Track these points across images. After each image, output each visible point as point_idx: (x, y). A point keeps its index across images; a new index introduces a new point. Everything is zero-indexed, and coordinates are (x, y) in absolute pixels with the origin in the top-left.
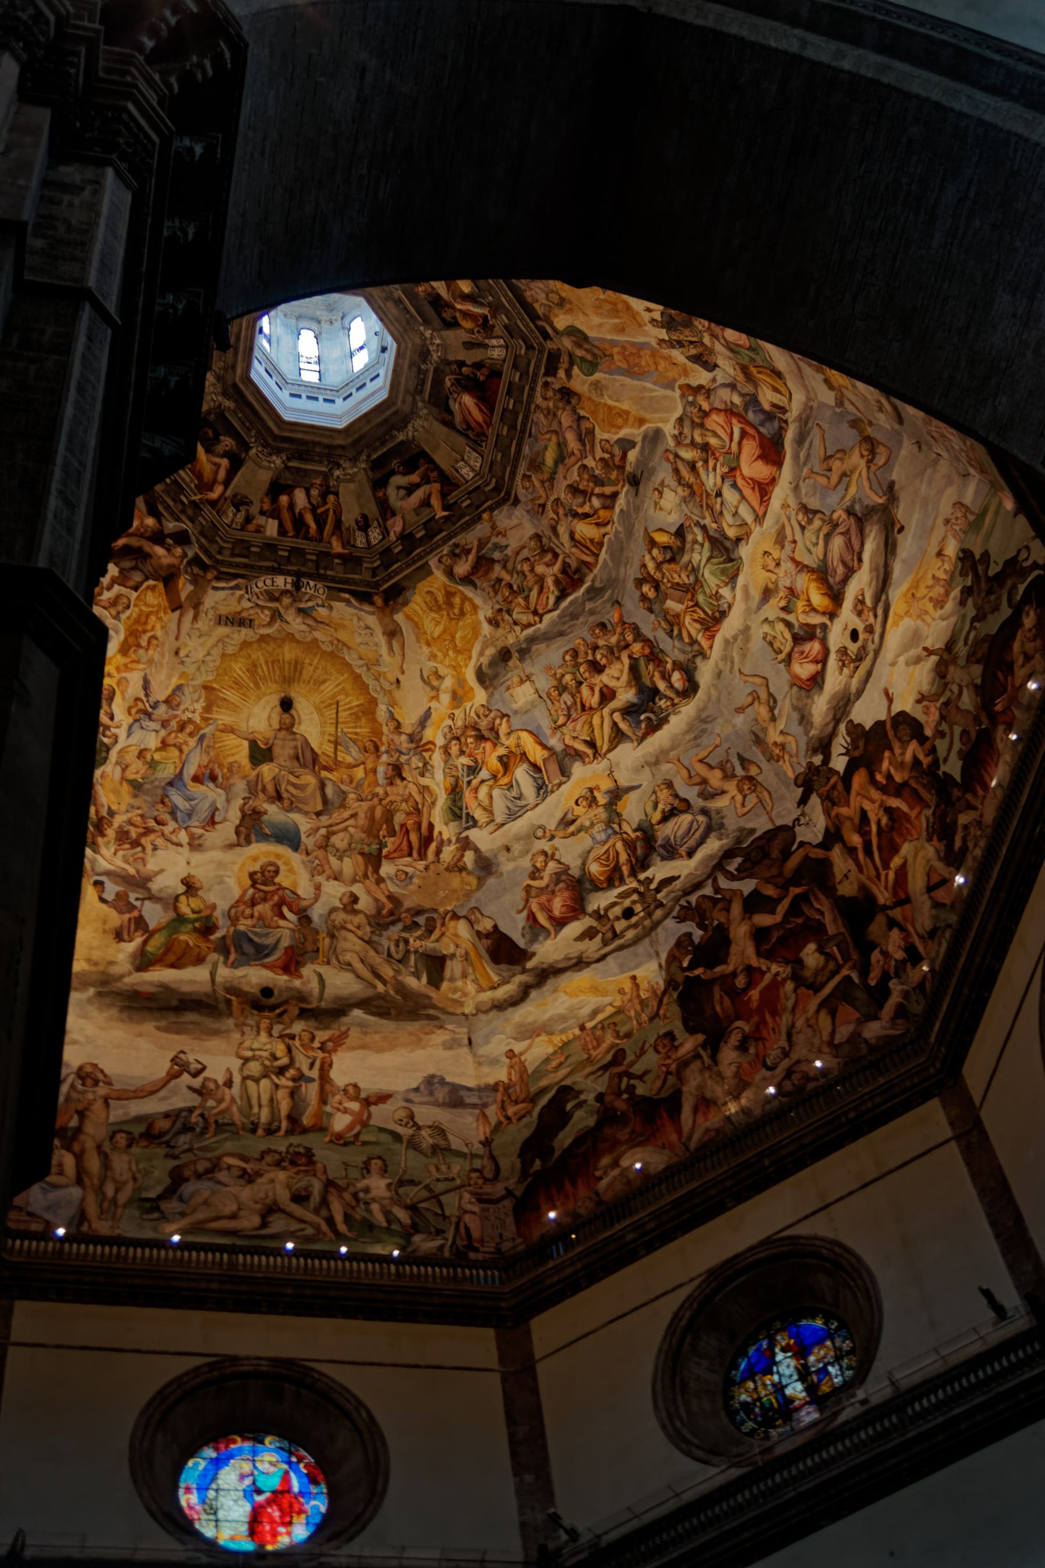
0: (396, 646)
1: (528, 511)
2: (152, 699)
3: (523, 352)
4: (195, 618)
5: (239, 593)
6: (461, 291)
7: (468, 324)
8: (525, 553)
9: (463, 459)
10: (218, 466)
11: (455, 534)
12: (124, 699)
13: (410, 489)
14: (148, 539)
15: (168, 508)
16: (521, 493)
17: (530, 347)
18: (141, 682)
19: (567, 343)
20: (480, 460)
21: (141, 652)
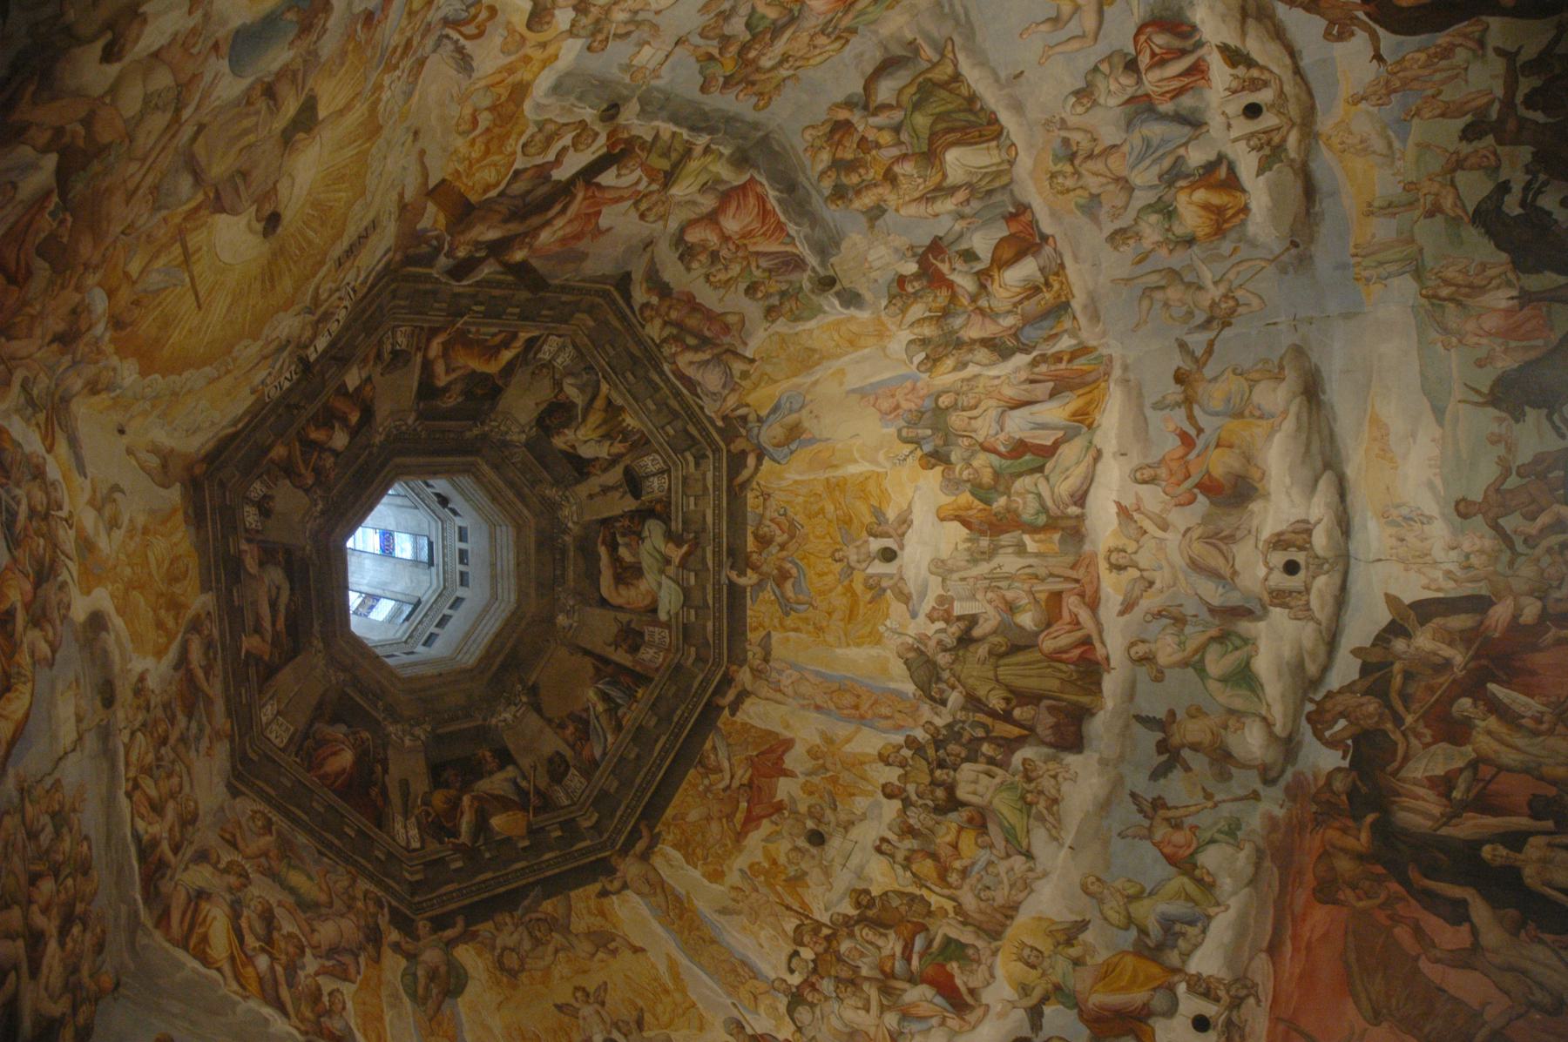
0: (154, 462)
1: (222, 809)
2: (450, 47)
3: (406, 875)
4: (401, 195)
5: (363, 275)
6: (492, 815)
7: (439, 799)
8: (187, 789)
9: (279, 713)
10: (447, 372)
11: (224, 659)
12: (509, 23)
13: (273, 605)
14: (516, 236)
15: (499, 284)
16: (247, 806)
17: (415, 888)
18: (475, 64)
19: (431, 956)
20: (277, 742)
21: (487, 102)
